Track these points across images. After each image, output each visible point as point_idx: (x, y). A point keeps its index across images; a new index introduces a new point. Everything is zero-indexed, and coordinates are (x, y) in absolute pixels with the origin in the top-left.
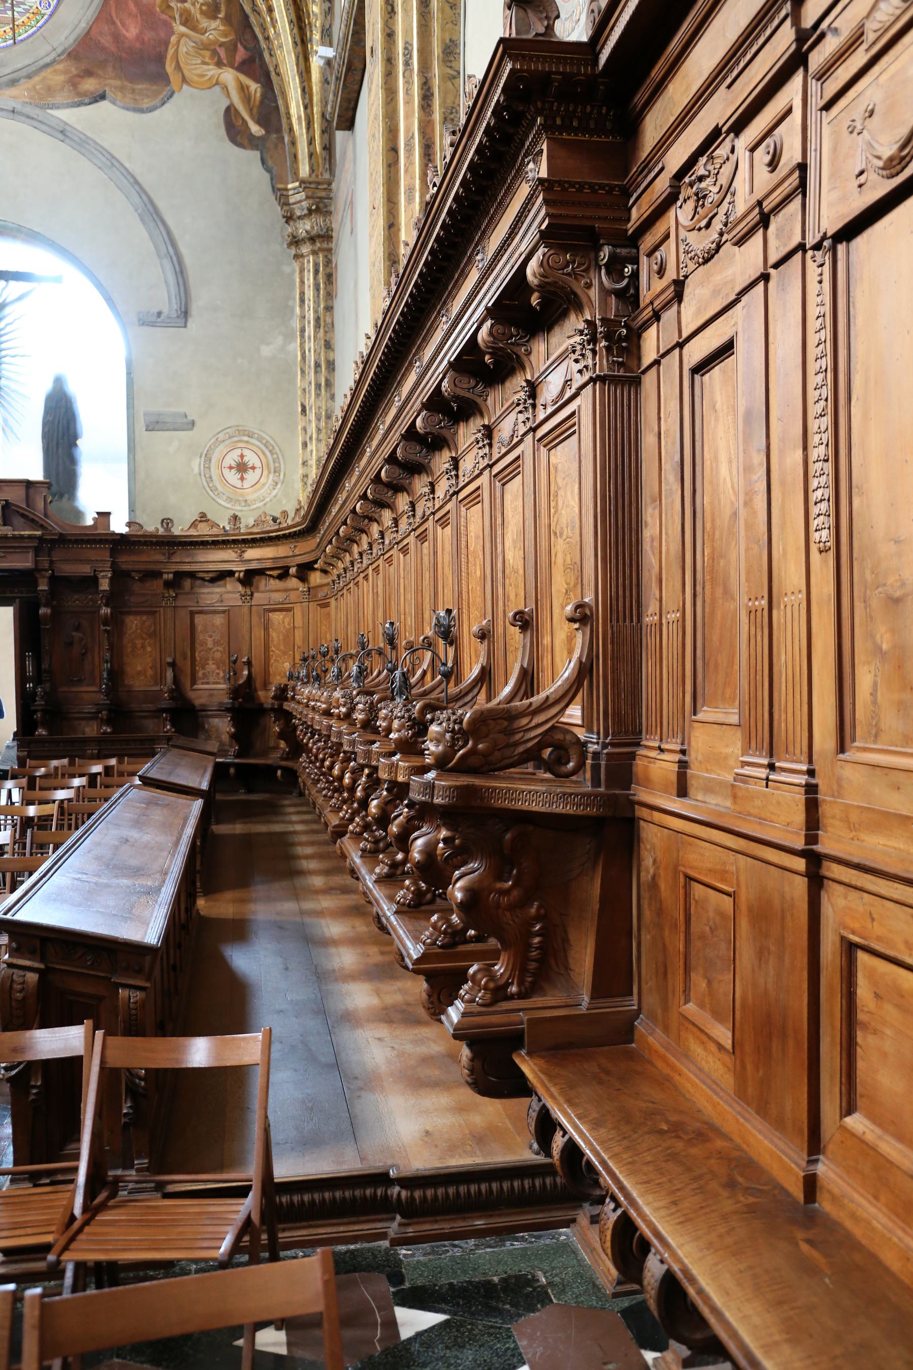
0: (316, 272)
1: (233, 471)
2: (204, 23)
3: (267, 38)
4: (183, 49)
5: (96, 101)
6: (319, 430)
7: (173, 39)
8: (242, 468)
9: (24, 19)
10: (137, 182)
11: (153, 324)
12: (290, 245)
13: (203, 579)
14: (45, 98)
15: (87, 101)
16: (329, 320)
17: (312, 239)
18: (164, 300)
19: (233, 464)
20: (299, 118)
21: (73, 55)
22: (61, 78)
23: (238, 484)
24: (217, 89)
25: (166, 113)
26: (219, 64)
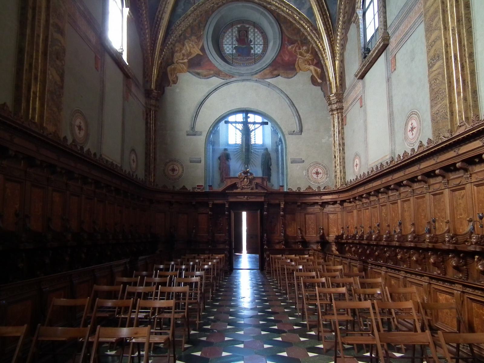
0: (338, 118)
1: (315, 174)
2: (305, 54)
3: (323, 57)
4: (300, 62)
5: (277, 76)
6: (340, 162)
7: (297, 59)
8: (317, 173)
9: (257, 58)
10: (288, 97)
11: (292, 134)
12: (329, 112)
13: (308, 204)
14: (264, 77)
15: (275, 76)
16: (343, 132)
17: (337, 110)
18: (296, 128)
19: (315, 172)
20: (333, 77)
21: (270, 65)
22: (268, 71)
23: (316, 178)
24: (309, 71)
25: (295, 78)
26: (309, 65)
